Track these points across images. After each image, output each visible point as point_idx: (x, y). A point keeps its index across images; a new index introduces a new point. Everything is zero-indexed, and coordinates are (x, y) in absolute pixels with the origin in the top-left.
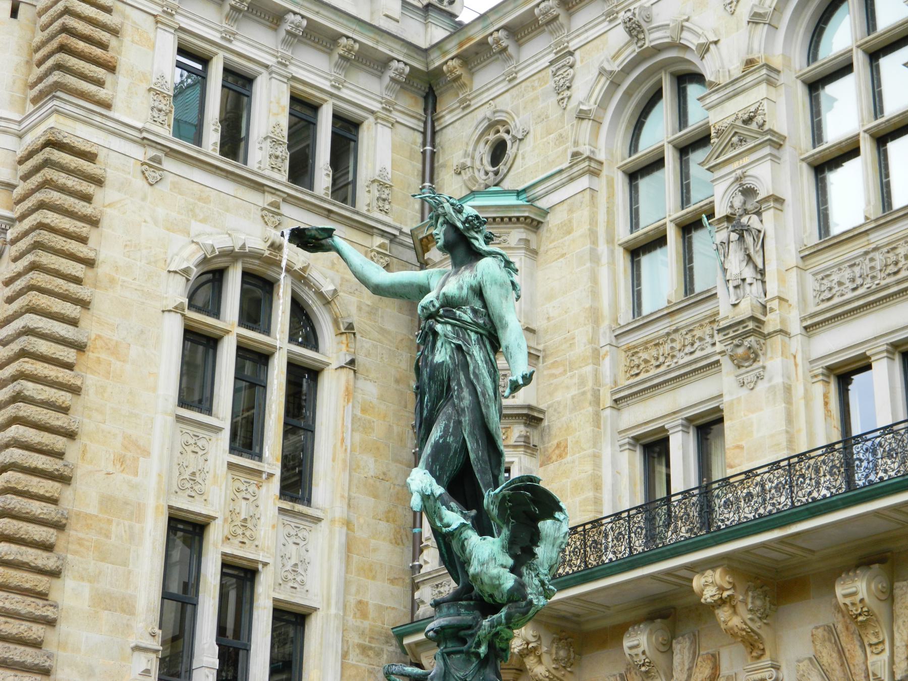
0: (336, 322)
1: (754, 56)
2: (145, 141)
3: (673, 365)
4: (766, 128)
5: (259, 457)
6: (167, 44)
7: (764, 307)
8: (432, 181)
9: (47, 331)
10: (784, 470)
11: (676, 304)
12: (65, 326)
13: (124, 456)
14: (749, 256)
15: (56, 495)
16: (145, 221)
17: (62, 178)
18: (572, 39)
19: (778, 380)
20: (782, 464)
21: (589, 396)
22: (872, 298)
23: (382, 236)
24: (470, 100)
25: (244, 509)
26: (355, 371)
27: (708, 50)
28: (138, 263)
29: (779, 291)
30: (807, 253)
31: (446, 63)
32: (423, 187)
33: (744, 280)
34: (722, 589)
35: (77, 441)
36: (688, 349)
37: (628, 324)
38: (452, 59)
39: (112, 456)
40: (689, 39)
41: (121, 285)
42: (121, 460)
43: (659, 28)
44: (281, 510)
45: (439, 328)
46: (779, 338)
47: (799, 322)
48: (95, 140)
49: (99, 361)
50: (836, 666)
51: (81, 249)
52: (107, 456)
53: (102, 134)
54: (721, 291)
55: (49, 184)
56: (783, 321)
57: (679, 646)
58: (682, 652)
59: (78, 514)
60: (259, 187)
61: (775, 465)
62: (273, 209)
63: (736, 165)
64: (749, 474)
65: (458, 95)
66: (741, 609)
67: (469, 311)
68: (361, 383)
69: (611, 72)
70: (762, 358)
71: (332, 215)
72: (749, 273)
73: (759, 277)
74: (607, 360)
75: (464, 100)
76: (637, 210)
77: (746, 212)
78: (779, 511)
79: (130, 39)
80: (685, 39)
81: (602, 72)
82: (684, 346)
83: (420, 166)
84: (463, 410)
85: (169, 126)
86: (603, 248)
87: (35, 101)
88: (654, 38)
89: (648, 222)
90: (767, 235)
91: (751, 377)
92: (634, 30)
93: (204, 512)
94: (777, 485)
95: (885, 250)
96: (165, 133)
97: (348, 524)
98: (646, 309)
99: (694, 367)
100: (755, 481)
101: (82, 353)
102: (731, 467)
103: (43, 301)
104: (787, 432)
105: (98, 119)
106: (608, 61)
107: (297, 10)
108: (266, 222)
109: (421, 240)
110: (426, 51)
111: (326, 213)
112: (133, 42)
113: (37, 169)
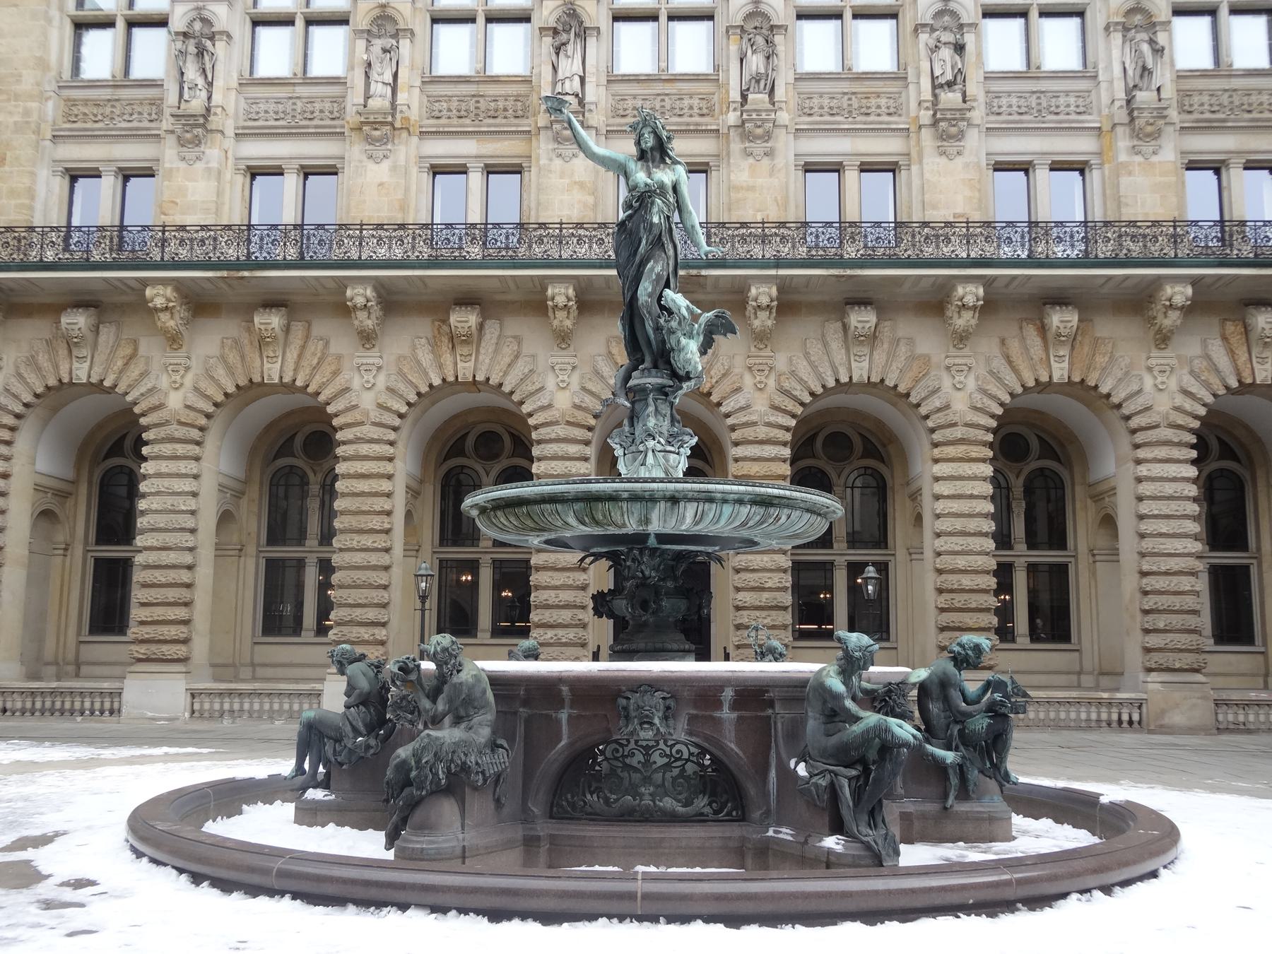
7: (208, 110)
14: (204, 70)
19: (214, 164)
21: (33, 126)
22: (294, 131)
34: (169, 300)
46: (219, 135)
50: (239, 366)
57: (106, 329)
58: (107, 334)
66: (177, 316)
70: (203, 146)
72: (200, 82)
74: (50, 104)
82: (124, 114)
86: (54, 13)
95: (304, 100)
99: (134, 133)
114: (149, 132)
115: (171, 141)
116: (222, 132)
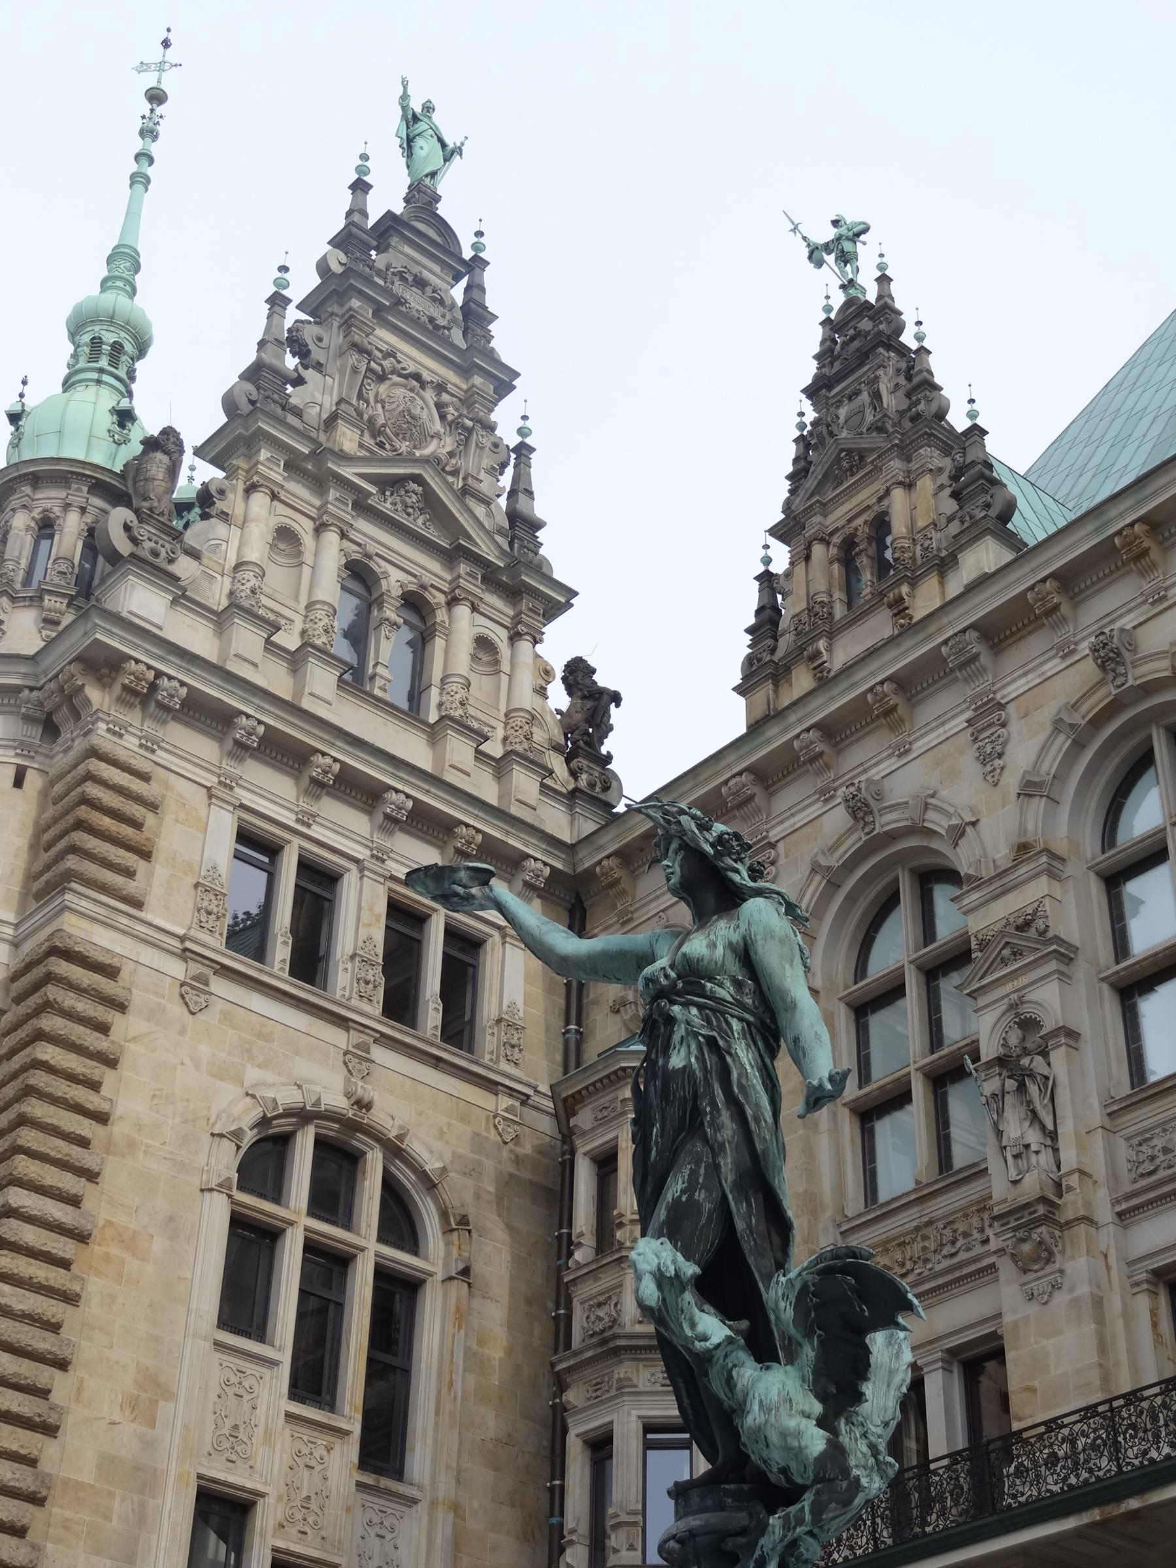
0: (444, 1214)
1: (1030, 838)
2: (188, 954)
3: (926, 1273)
4: (1050, 934)
5: (331, 1406)
6: (224, 826)
7: (1058, 1185)
8: (579, 1023)
9: (36, 1212)
10: (1104, 1418)
11: (928, 1185)
12: (62, 1205)
13: (138, 1397)
14: (1034, 1113)
15: (35, 1452)
16: (182, 1064)
17: (69, 1000)
18: (773, 827)
19: (1084, 1290)
20: (1101, 1409)
23: (511, 1096)
24: (632, 913)
25: (307, 1482)
26: (469, 1285)
27: (963, 834)
28: (170, 1121)
29: (1079, 1162)
30: (1116, 1107)
31: (600, 862)
32: (568, 1031)
33: (1027, 1146)
35: (71, 1372)
36: (947, 1250)
37: (860, 1215)
38: (608, 857)
39: (120, 1397)
40: (937, 821)
41: (145, 1152)
42: (133, 1404)
43: (893, 808)
44: (360, 1485)
45: (676, 1009)
46: (1081, 1229)
47: (1109, 1206)
48: (118, 950)
49: (107, 1258)
51: (91, 1098)
52: (113, 1397)
53: (128, 941)
54: (994, 1165)
55: (52, 1007)
56: (1088, 1204)
59: (66, 1482)
60: (342, 1022)
61: (1089, 1411)
62: (360, 1053)
63: (1009, 988)
64: (1052, 1425)
65: (615, 907)
67: (728, 984)
68: (477, 1303)
69: (829, 868)
70: (1058, 1258)
71: (441, 1065)
72: (1033, 1137)
73: (1049, 1142)
75: (621, 914)
76: (868, 1057)
77: (1026, 1052)
78: (1098, 1479)
79: (173, 816)
80: (932, 822)
81: (815, 868)
82: (942, 1245)
83: (562, 1002)
84: (722, 1146)
85: (221, 934)
87: (38, 896)
88: (888, 821)
89: (882, 1073)
90: (1057, 1083)
91: (1043, 1285)
92: (859, 810)
93: (249, 1484)
94: (1095, 1440)
96: (214, 943)
97: (456, 1508)
98: (884, 1195)
99: (957, 1274)
100: (1060, 1436)
101: (84, 1246)
102: (1020, 1419)
103: (33, 1168)
104: (1100, 1365)
105: (124, 920)
106: (824, 854)
107: (399, 786)
108: (349, 1071)
109: (565, 1100)
110: (573, 846)
111: (434, 1061)
112: (177, 820)
113: (37, 987)
114: (979, 1265)
115: (1006, 1268)
116: (1089, 1220)
